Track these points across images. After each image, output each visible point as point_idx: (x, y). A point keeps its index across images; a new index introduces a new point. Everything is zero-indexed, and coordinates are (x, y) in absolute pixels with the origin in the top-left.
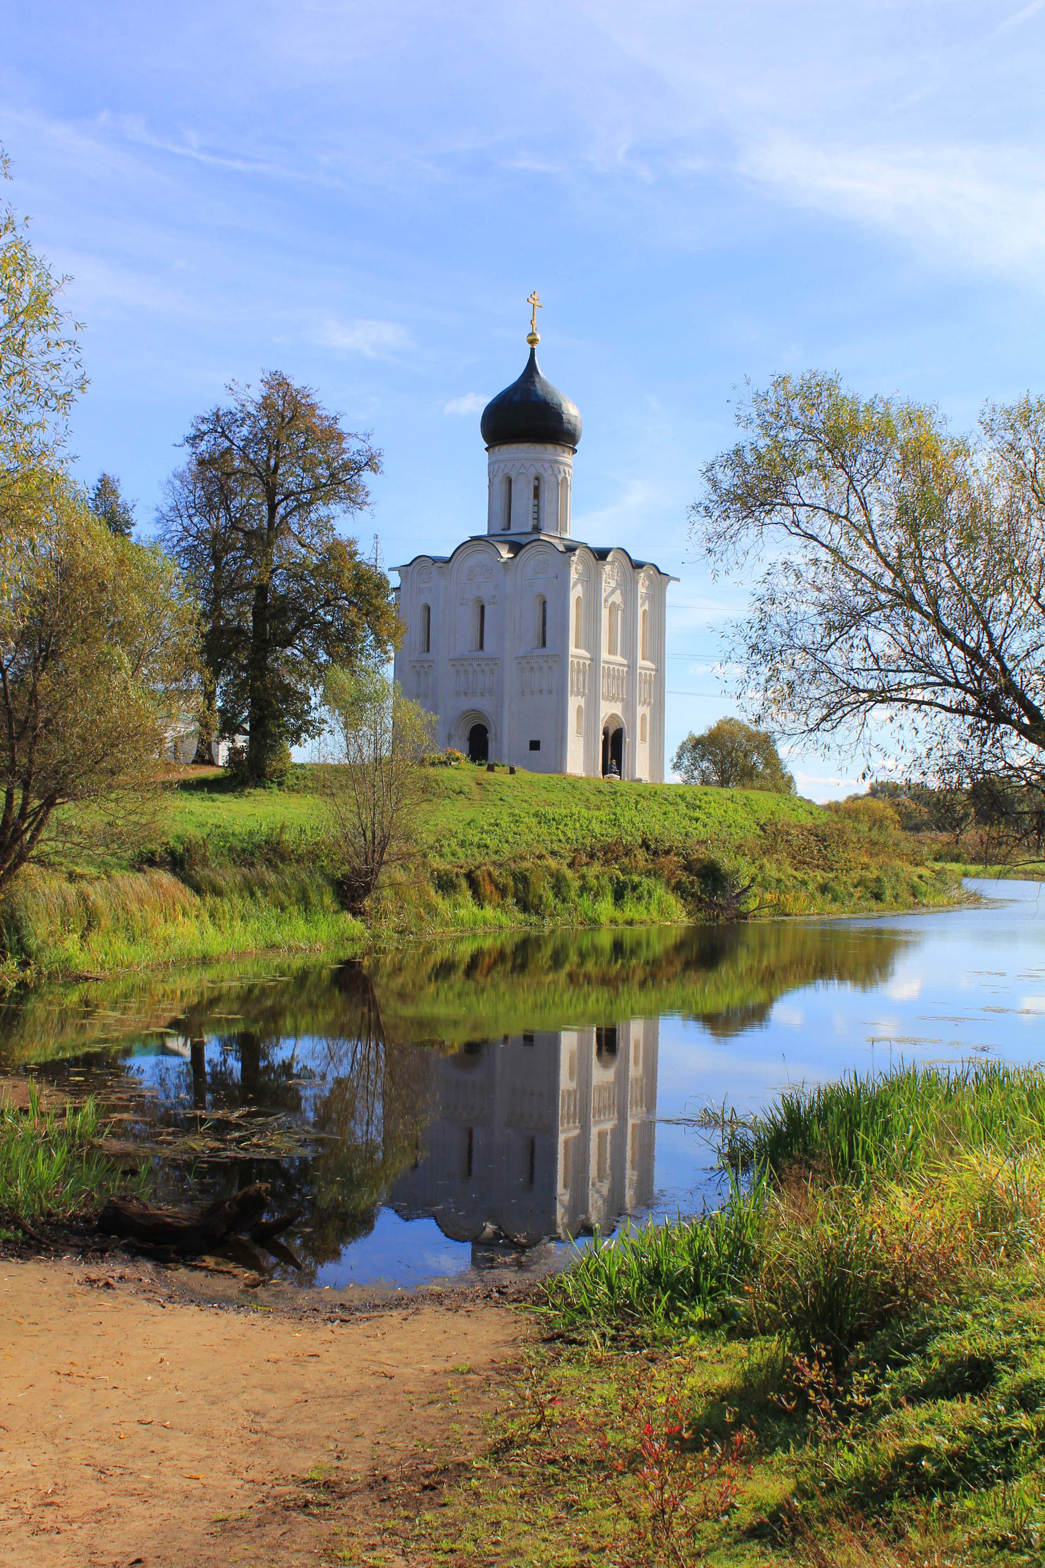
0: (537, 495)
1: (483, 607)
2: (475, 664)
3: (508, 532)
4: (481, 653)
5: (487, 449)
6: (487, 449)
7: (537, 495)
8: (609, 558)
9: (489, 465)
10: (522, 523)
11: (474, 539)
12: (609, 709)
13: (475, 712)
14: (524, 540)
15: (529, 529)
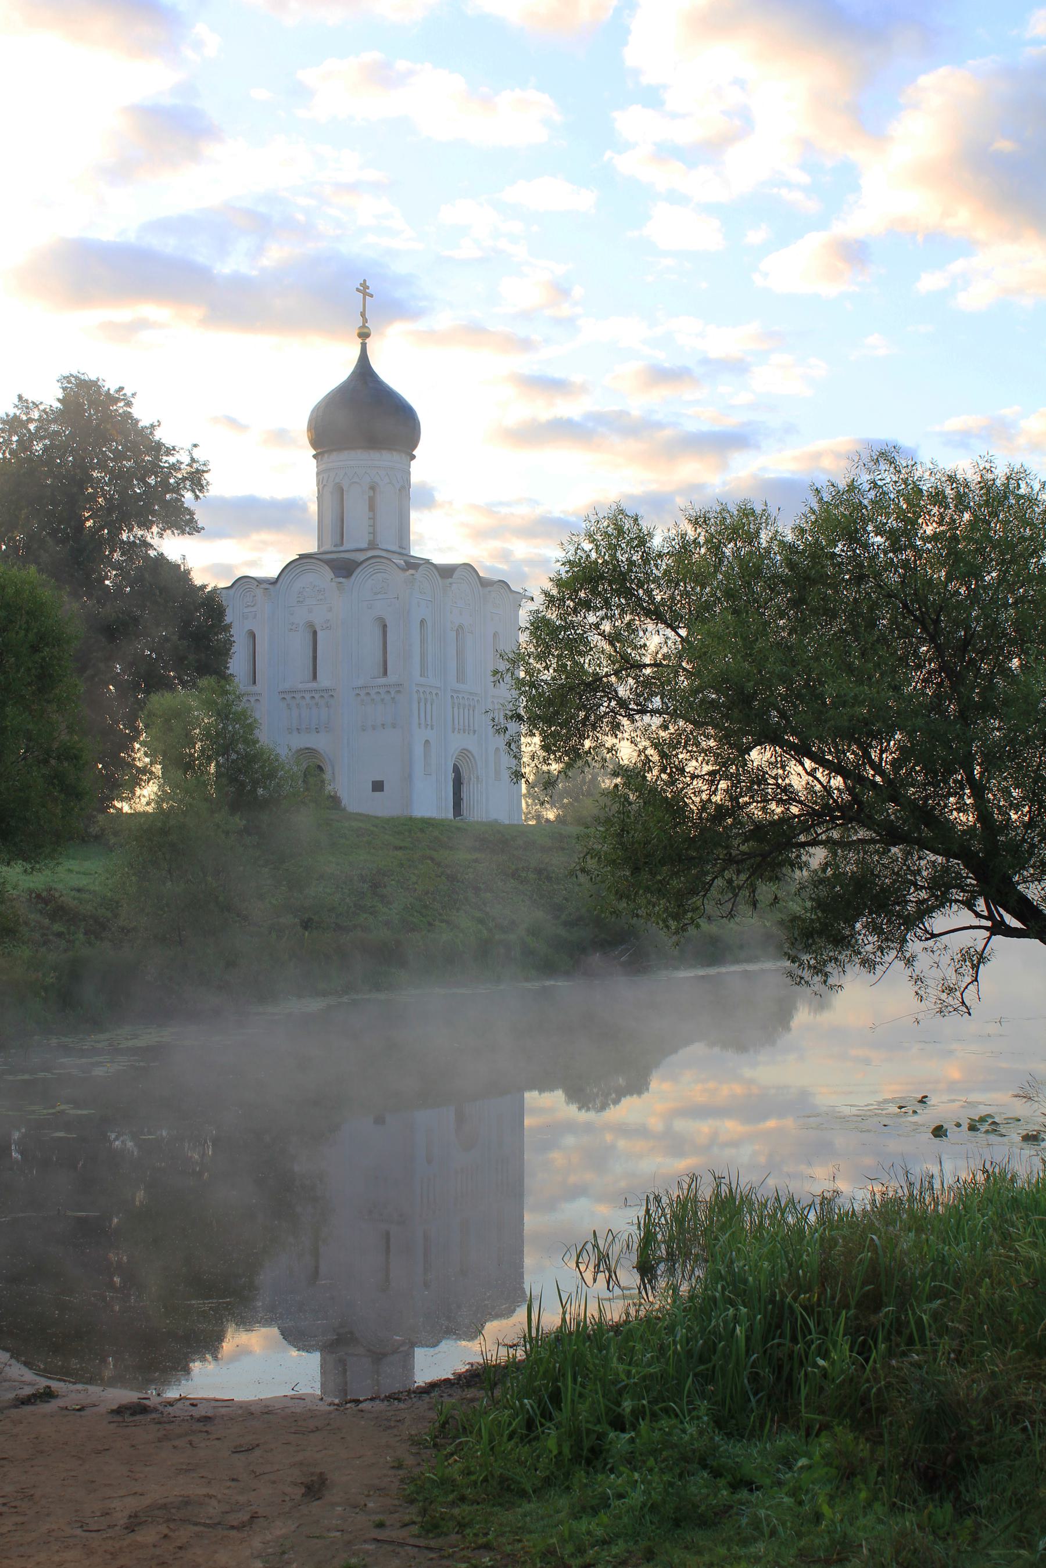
0: (372, 508)
1: (315, 633)
2: (308, 696)
3: (342, 549)
4: (314, 685)
5: (314, 456)
6: (314, 456)
7: (372, 508)
8: (456, 575)
9: (318, 474)
10: (357, 537)
11: (302, 557)
12: (458, 742)
13: (310, 752)
14: (360, 557)
15: (364, 545)
